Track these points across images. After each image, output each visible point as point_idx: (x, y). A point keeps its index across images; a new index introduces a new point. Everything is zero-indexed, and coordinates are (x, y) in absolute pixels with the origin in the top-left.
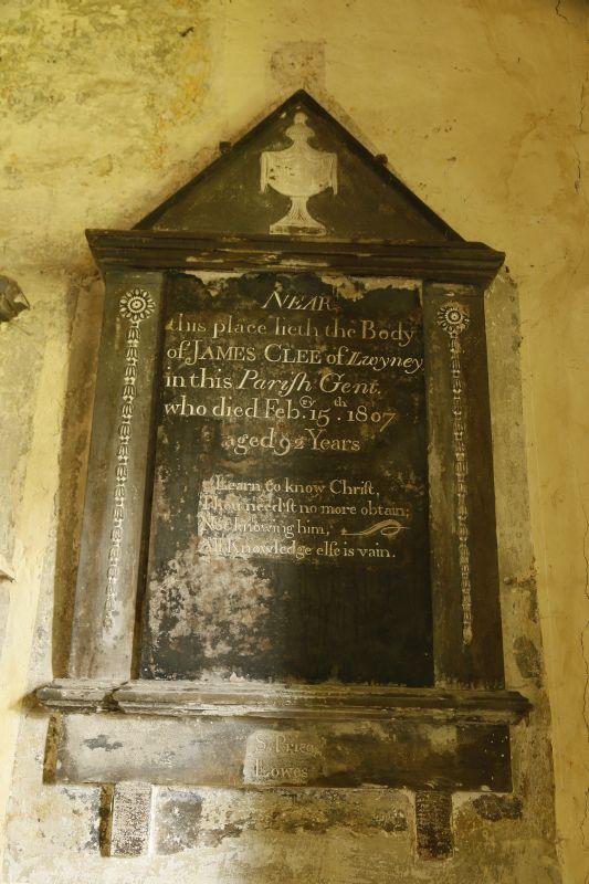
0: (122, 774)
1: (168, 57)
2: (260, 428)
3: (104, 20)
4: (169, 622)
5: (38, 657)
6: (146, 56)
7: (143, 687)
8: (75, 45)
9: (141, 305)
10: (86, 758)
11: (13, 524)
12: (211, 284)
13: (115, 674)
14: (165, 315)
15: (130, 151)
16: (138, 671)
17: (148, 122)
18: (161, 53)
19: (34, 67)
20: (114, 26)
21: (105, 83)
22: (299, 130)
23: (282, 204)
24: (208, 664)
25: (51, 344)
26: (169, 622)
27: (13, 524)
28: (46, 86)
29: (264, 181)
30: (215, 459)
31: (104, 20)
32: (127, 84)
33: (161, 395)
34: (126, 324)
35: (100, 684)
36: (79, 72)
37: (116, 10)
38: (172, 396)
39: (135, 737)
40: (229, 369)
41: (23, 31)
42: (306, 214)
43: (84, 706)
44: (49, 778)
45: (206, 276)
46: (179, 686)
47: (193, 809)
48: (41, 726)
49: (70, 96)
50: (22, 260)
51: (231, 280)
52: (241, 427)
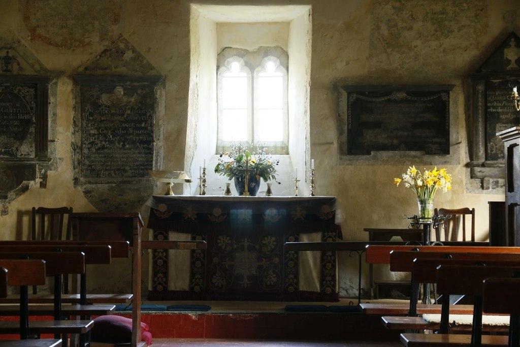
0: (485, 176)
1: (478, 17)
2: (507, 113)
3: (462, 8)
4: (492, 151)
5: (466, 158)
6: (472, 17)
7: (488, 162)
8: (456, 16)
9: (481, 88)
10: (479, 174)
11: (458, 133)
12: (496, 83)
13: (482, 160)
14: (486, 90)
15: (471, 44)
16: (486, 159)
17: (474, 36)
18: (476, 16)
19: (447, 23)
20: (465, 9)
21: (463, 26)
22: (513, 43)
23: (509, 62)
24: (499, 158)
25: (460, 95)
26: (492, 151)
27: (458, 133)
28: (449, 28)
29: (505, 56)
30: (499, 120)
31: (462, 8)
32: (469, 26)
33: (486, 108)
34: (478, 91)
35: (482, 160)
36: (457, 24)
37: (465, 5)
38: (489, 107)
39: (486, 170)
40: (501, 102)
41: (443, 13)
42: (515, 64)
43: (478, 166)
44: (472, 177)
45: (494, 81)
46: (495, 162)
47: (497, 182)
48: (469, 169)
49: (456, 30)
50: (451, 74)
51: (500, 82)
52: (503, 113)
